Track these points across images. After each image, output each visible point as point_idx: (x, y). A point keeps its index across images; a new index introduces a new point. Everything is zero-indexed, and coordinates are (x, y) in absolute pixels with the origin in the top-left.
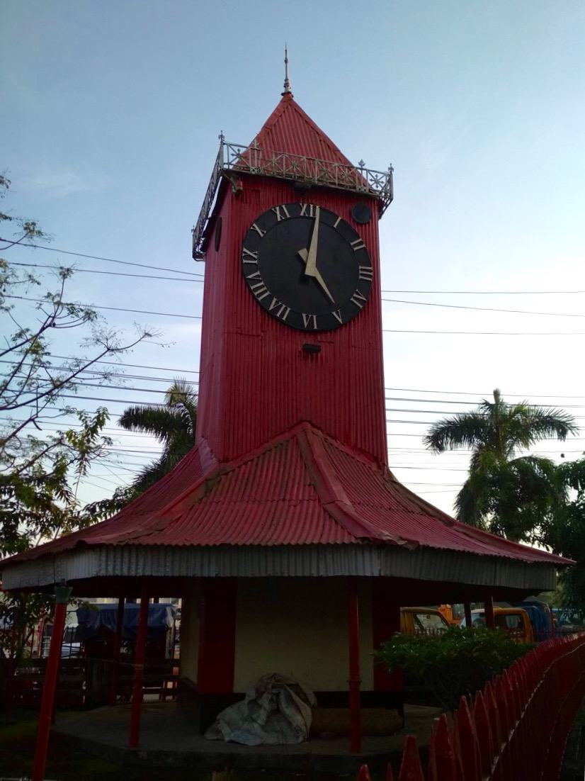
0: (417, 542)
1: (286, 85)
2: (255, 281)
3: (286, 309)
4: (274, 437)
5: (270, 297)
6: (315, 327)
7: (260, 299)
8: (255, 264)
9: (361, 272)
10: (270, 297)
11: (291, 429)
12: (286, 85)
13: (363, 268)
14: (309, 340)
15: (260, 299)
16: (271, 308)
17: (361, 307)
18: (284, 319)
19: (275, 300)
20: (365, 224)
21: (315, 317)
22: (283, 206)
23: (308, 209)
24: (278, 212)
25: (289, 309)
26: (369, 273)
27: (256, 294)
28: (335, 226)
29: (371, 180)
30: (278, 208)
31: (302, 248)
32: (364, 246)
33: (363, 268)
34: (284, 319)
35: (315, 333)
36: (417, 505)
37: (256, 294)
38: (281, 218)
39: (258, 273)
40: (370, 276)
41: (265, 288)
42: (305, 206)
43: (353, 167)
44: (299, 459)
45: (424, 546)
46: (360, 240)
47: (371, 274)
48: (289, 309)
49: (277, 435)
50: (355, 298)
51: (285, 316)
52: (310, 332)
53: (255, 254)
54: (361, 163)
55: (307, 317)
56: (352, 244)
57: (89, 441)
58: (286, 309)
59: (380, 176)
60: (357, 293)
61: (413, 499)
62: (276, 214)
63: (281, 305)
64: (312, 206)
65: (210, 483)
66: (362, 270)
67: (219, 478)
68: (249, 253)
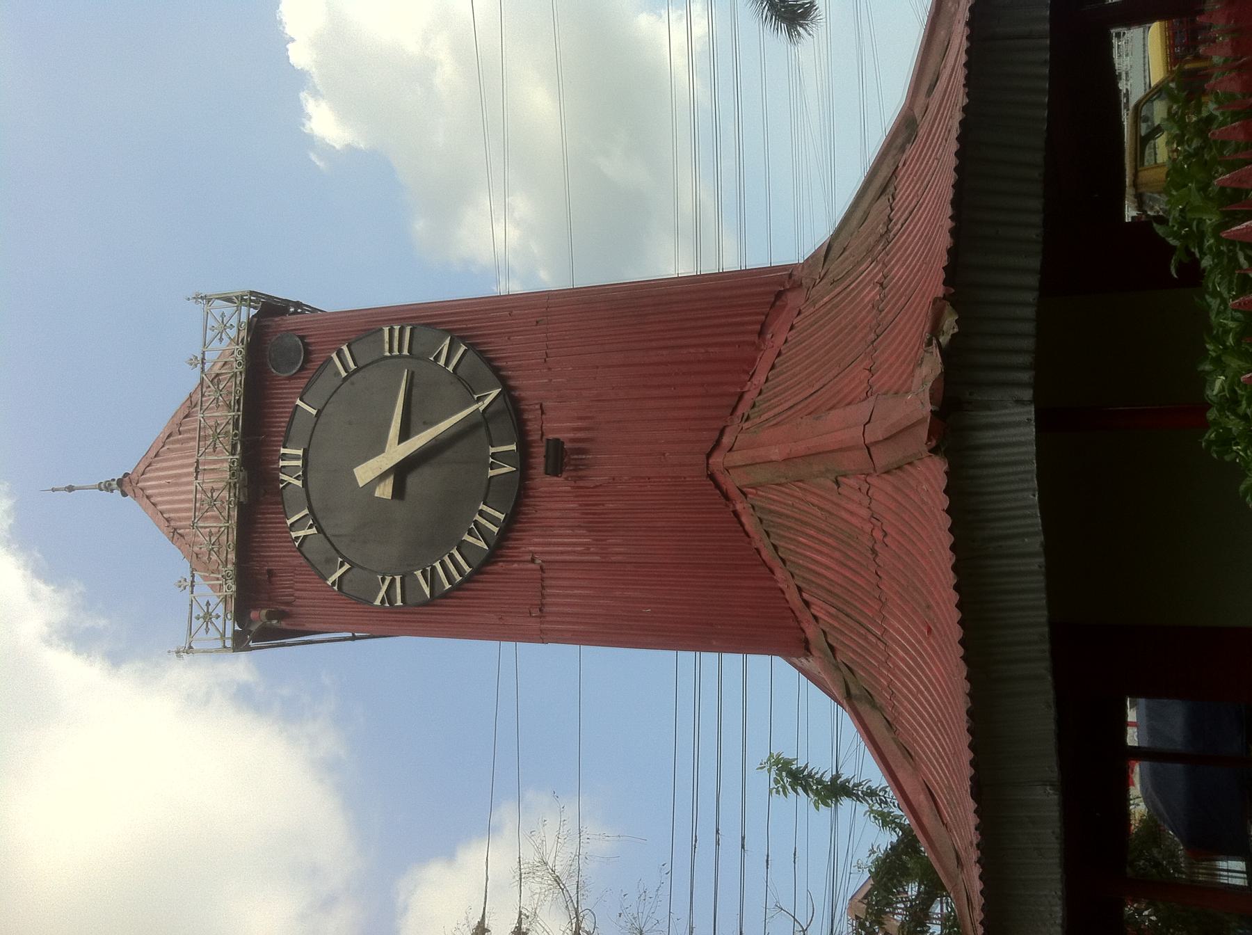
0: (935, 300)
1: (107, 487)
2: (433, 580)
3: (481, 513)
4: (747, 535)
5: (461, 546)
7: (467, 569)
8: (402, 579)
9: (396, 353)
11: (726, 496)
12: (107, 487)
13: (387, 346)
14: (539, 461)
15: (467, 569)
16: (482, 544)
17: (463, 348)
18: (502, 517)
19: (467, 538)
20: (308, 344)
21: (492, 450)
22: (289, 522)
25: (482, 507)
26: (396, 334)
27: (458, 578)
29: (221, 339)
30: (294, 535)
32: (345, 348)
36: (871, 205)
38: (311, 527)
39: (418, 573)
41: (446, 559)
43: (202, 380)
44: (780, 488)
45: (945, 283)
47: (397, 328)
48: (482, 507)
49: (742, 525)
50: (447, 363)
51: (497, 514)
52: (523, 458)
53: (383, 580)
54: (192, 362)
55: (492, 466)
57: (820, 781)
58: (481, 513)
59: (211, 322)
60: (437, 358)
61: (859, 214)
62: (305, 537)
63: (476, 523)
64: (282, 463)
65: (854, 691)
66: (391, 350)
67: (844, 669)
68: (382, 594)
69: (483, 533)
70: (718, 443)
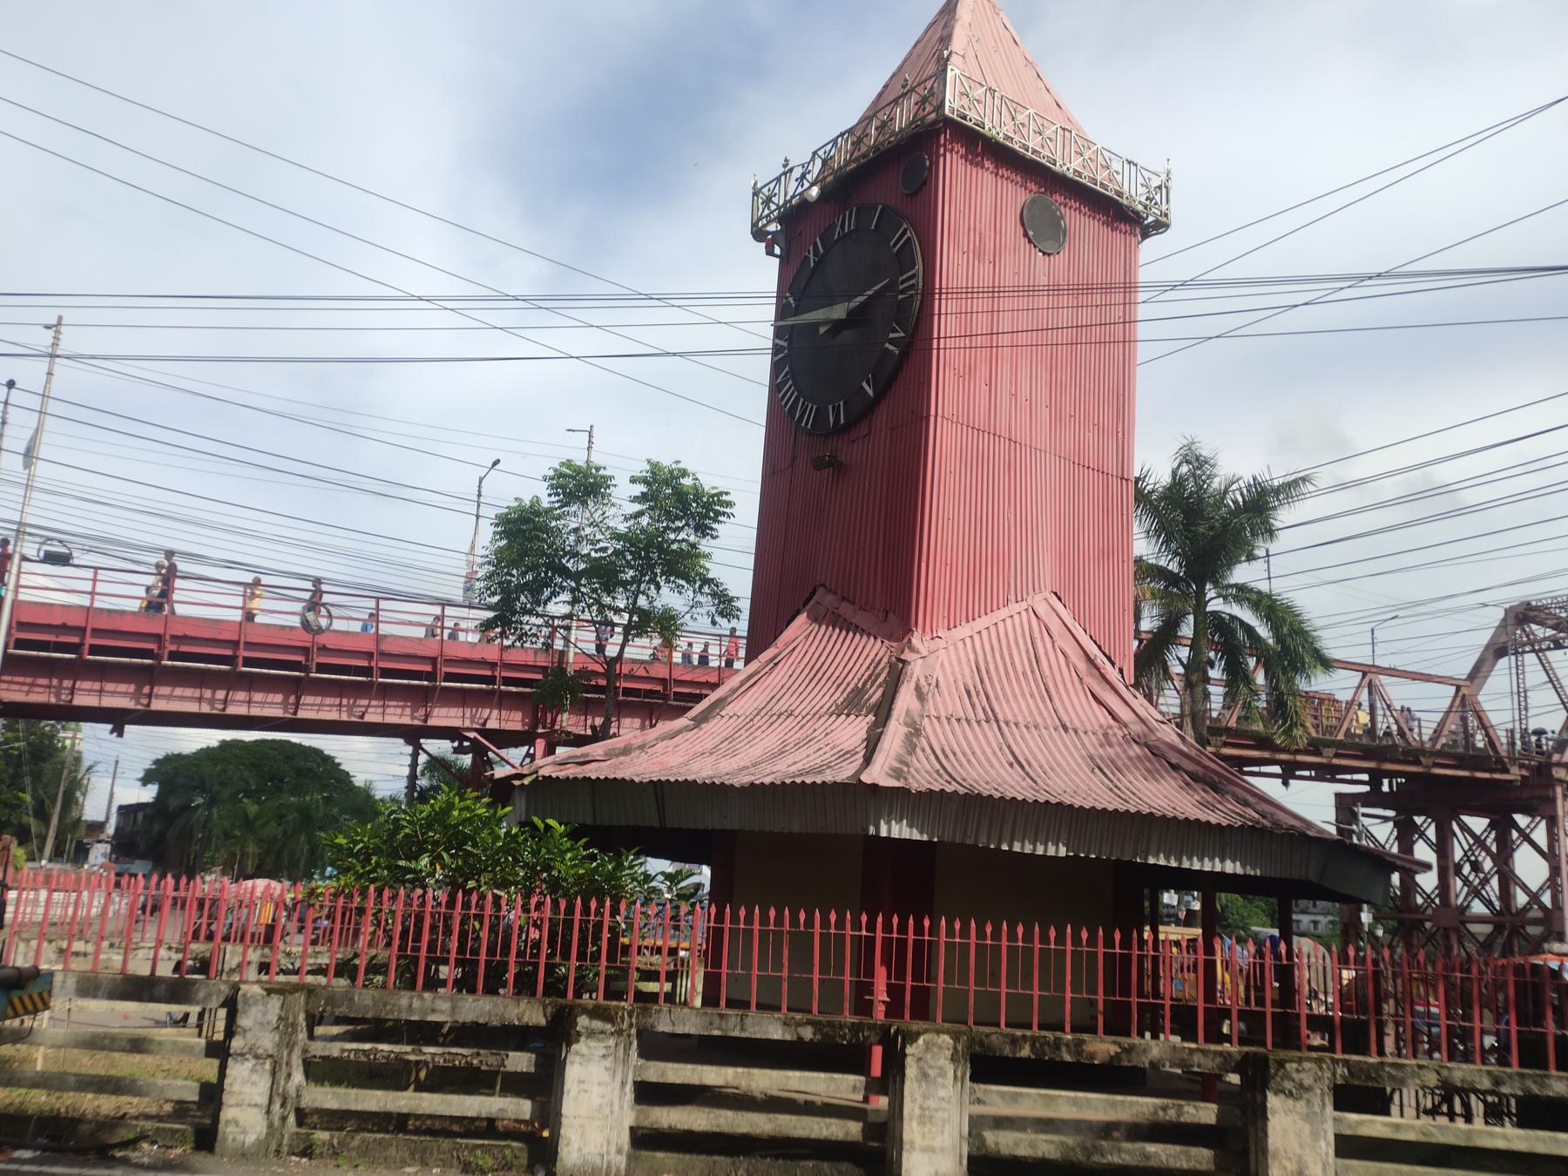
6: (842, 422)
13: (904, 277)
18: (809, 427)
19: (802, 400)
27: (783, 403)
30: (811, 248)
33: (904, 277)
34: (809, 427)
35: (849, 426)
63: (807, 406)
64: (847, 213)
70: (830, 591)
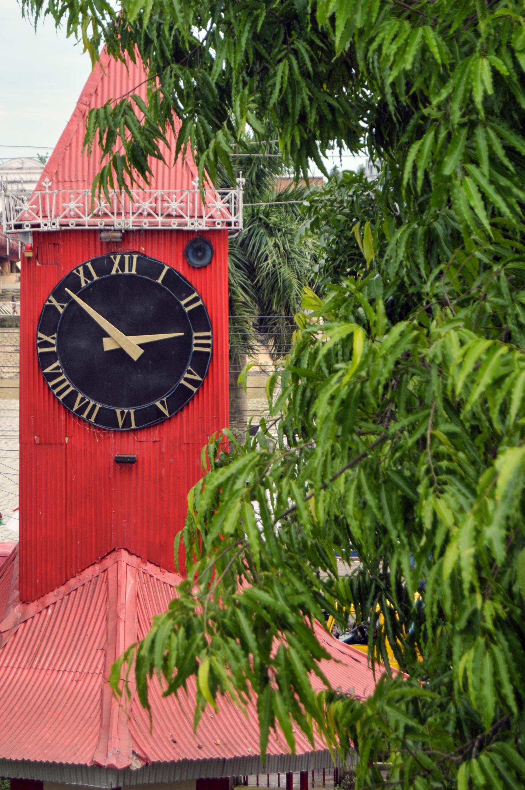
5: (73, 394)
8: (53, 352)
10: (73, 394)
11: (104, 558)
23: (122, 265)
24: (82, 275)
27: (56, 391)
28: (159, 281)
31: (102, 342)
37: (56, 391)
40: (207, 346)
42: (119, 257)
46: (195, 295)
50: (186, 380)
56: (183, 303)
60: (189, 372)
69: (81, 410)
